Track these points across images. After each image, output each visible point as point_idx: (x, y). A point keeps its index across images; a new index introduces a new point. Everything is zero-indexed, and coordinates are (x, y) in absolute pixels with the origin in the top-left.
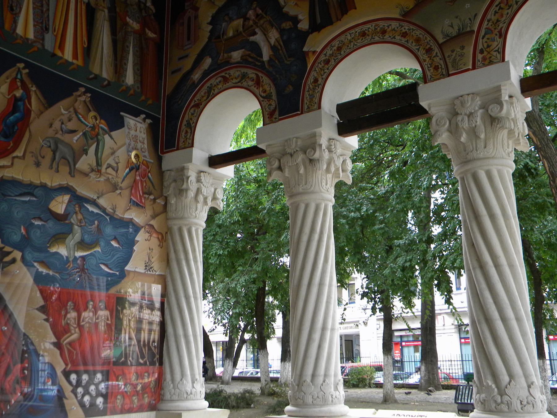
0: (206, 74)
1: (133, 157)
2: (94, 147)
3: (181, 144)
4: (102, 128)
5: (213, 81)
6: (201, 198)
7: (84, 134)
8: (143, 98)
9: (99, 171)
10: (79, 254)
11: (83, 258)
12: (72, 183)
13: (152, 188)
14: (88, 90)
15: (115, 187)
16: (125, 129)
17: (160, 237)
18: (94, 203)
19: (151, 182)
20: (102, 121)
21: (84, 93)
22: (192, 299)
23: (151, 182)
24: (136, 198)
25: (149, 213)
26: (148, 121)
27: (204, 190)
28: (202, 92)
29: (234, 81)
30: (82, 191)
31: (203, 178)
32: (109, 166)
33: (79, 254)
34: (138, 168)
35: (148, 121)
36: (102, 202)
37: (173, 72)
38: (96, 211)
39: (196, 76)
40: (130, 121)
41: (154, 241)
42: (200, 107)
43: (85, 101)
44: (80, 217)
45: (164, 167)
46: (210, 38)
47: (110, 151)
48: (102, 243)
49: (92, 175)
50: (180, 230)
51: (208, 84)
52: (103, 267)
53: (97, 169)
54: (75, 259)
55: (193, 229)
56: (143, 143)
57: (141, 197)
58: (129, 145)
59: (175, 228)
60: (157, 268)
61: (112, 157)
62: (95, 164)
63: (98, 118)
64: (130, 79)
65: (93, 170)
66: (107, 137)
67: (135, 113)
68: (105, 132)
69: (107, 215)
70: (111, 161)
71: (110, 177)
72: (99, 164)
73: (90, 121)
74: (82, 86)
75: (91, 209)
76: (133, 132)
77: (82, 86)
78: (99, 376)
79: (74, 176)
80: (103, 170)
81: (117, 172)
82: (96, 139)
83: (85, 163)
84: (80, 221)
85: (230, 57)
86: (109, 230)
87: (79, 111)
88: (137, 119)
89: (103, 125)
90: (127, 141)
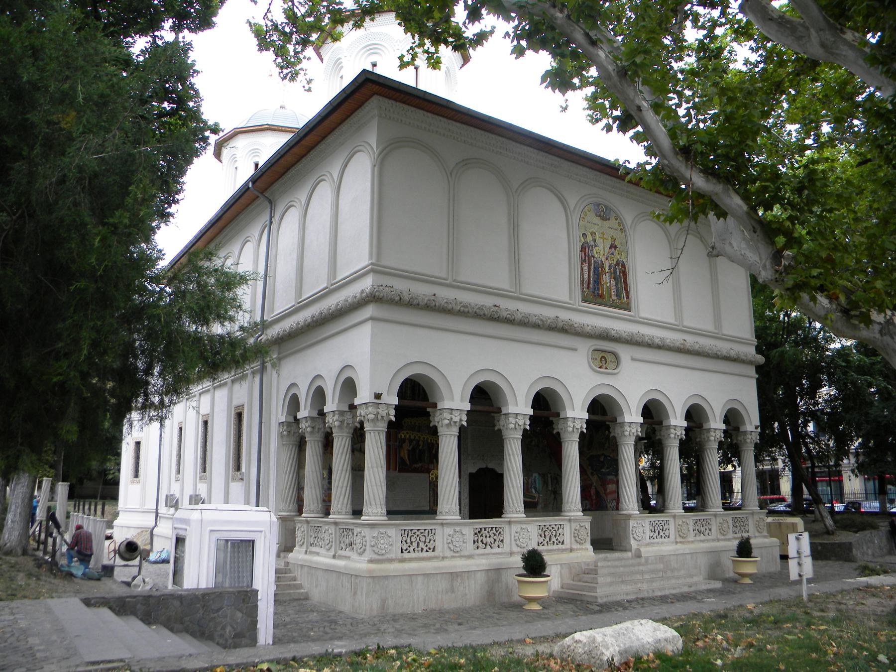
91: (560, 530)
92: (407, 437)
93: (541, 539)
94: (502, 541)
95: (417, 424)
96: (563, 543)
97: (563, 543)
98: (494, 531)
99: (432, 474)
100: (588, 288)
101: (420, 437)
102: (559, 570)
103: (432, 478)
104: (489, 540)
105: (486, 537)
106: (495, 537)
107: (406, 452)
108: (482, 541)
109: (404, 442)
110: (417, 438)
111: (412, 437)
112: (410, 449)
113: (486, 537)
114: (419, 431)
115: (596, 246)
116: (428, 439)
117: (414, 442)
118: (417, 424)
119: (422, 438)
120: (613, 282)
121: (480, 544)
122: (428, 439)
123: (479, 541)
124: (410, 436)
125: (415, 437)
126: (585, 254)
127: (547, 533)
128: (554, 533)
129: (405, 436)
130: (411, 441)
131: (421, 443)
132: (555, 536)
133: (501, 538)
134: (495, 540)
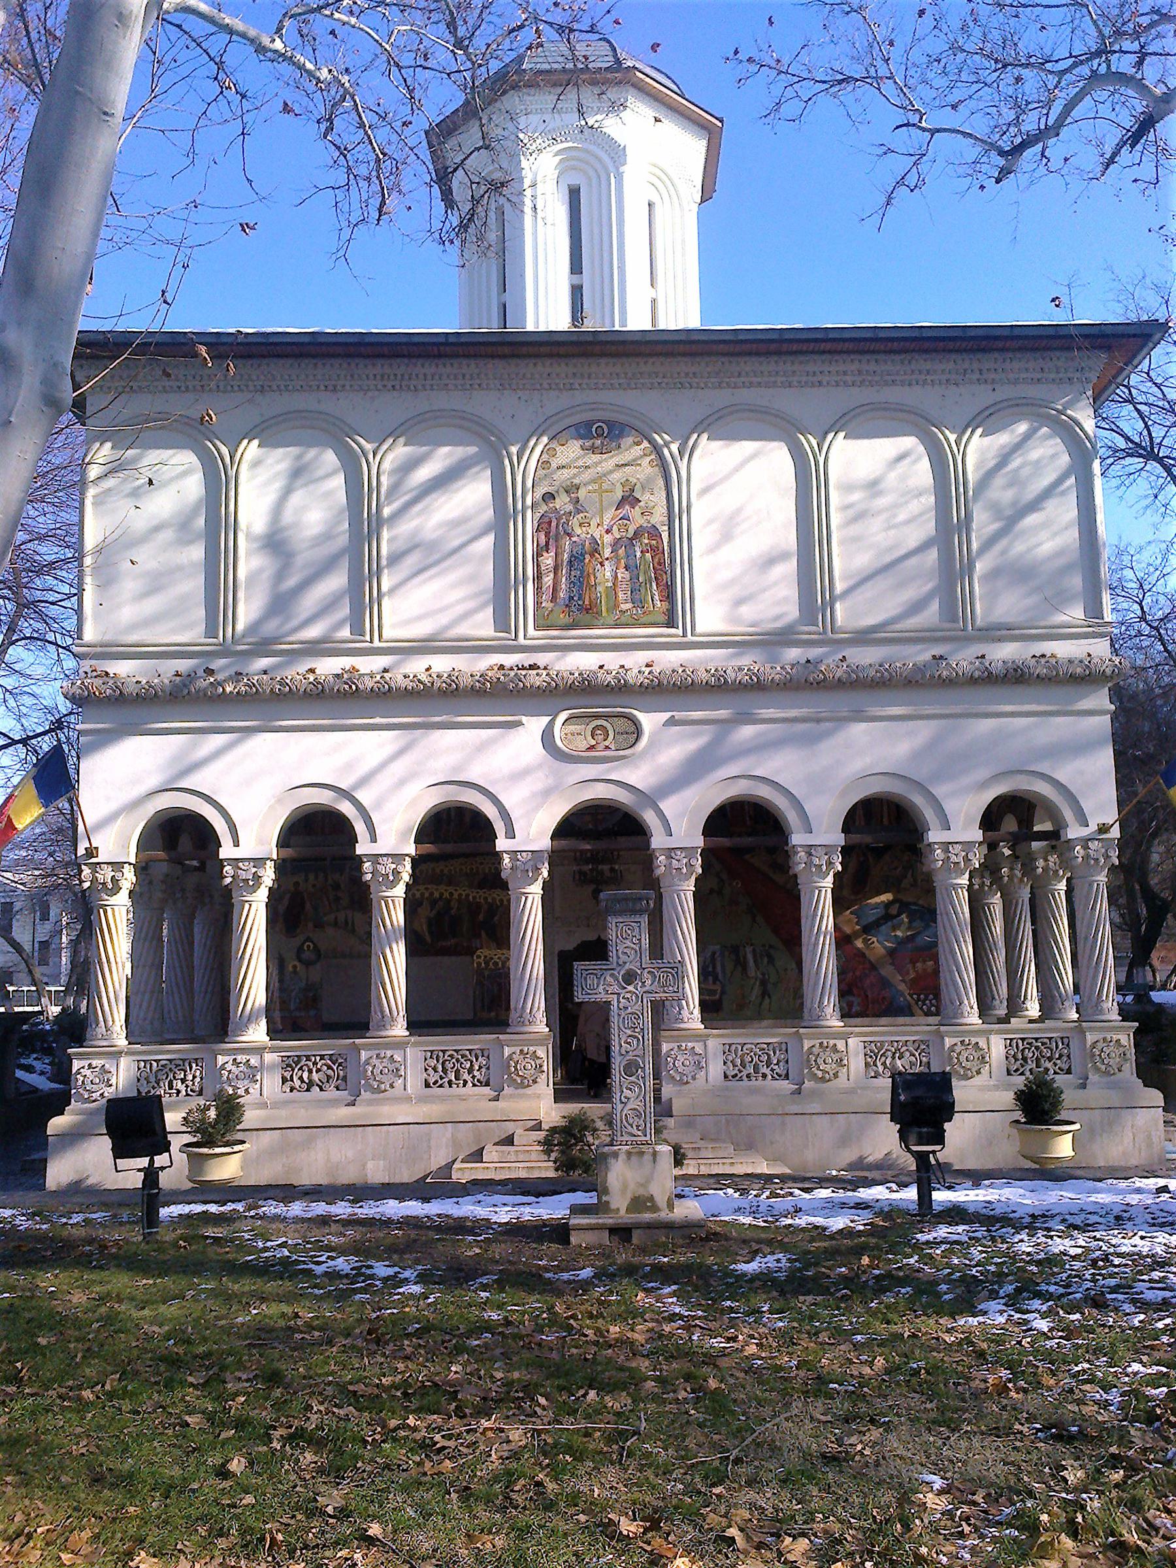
12: (900, 896)
18: (915, 904)
30: (905, 899)
36: (921, 902)
72: (915, 881)
78: (931, 996)
83: (905, 883)
92: (427, 895)
94: (345, 1079)
99: (479, 957)
100: (554, 598)
101: (451, 894)
102: (449, 1135)
103: (479, 964)
106: (330, 1072)
107: (423, 920)
109: (421, 904)
110: (446, 895)
111: (437, 895)
112: (432, 915)
114: (450, 883)
115: (579, 512)
116: (467, 895)
117: (441, 903)
118: (446, 871)
119: (456, 896)
120: (622, 574)
122: (467, 895)
124: (432, 894)
125: (441, 894)
126: (547, 535)
127: (449, 1065)
129: (422, 894)
130: (434, 903)
131: (454, 904)
132: (470, 1071)
134: (329, 1077)
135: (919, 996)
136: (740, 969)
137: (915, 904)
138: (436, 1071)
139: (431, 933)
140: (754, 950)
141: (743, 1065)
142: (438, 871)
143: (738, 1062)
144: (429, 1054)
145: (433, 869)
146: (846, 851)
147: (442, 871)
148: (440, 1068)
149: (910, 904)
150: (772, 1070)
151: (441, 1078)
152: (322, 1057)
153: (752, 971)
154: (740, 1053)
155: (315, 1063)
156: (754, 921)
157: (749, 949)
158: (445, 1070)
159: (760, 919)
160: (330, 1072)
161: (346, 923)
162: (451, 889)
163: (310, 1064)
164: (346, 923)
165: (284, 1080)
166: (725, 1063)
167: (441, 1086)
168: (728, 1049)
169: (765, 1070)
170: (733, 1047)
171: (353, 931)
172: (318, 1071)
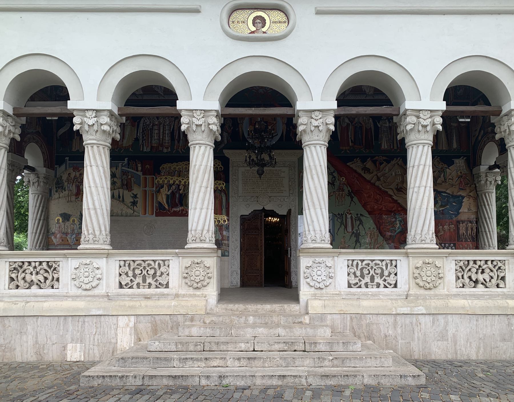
0: (482, 137)
1: (459, 173)
2: (442, 175)
3: (478, 164)
4: (445, 167)
5: (485, 139)
6: (488, 182)
7: (439, 171)
8: (462, 150)
9: (446, 182)
10: (441, 209)
11: (442, 210)
13: (468, 182)
14: (438, 156)
15: (452, 185)
16: (455, 164)
17: (474, 198)
19: (469, 180)
20: (445, 165)
21: (437, 158)
22: (488, 219)
23: (469, 180)
24: (462, 187)
25: (468, 191)
26: (465, 158)
27: (489, 179)
28: (482, 144)
29: (491, 139)
31: (488, 175)
32: (450, 179)
33: (441, 209)
34: (462, 177)
35: (465, 158)
37: (474, 136)
38: (446, 195)
39: (480, 138)
40: (456, 161)
41: (471, 200)
42: (482, 149)
43: (438, 161)
44: (440, 198)
45: (474, 173)
46: (482, 123)
47: (449, 174)
48: (449, 204)
49: (443, 184)
50: (482, 195)
51: (484, 141)
52: (450, 212)
53: (445, 181)
54: (440, 211)
55: (490, 194)
56: (463, 167)
57: (464, 186)
58: (457, 169)
59: (480, 195)
60: (474, 209)
61: (450, 176)
62: (444, 180)
63: (443, 164)
64: (455, 146)
65: (443, 182)
66: (447, 169)
67: (458, 157)
68: (447, 168)
69: (450, 195)
70: (450, 177)
71: (450, 182)
73: (441, 166)
74: (436, 156)
75: (444, 194)
76: (458, 165)
77: (436, 156)
79: (436, 186)
80: (447, 181)
81: (453, 180)
82: (443, 172)
84: (440, 199)
85: (488, 130)
86: (451, 200)
87: (436, 164)
88: (460, 159)
89: (446, 166)
90: (456, 168)
91: (163, 269)
93: (125, 280)
94: (58, 280)
95: (177, 169)
96: (167, 286)
97: (167, 286)
98: (44, 265)
102: (132, 324)
104: (34, 277)
105: (31, 273)
106: (46, 275)
108: (24, 278)
113: (31, 273)
121: (21, 283)
123: (20, 278)
127: (137, 272)
128: (152, 272)
130: (170, 186)
133: (56, 276)
134: (46, 279)
135: (445, 244)
136: (343, 227)
137: (445, 192)
138: (128, 276)
139: (167, 202)
140: (351, 217)
141: (362, 276)
142: (172, 168)
143: (358, 273)
144: (122, 263)
145: (170, 168)
146: (445, 116)
147: (175, 168)
148: (130, 273)
149: (443, 192)
150: (385, 280)
151: (131, 281)
152: (41, 263)
153: (350, 229)
154: (360, 267)
155: (35, 267)
156: (352, 200)
157: (349, 216)
158: (135, 276)
159: (355, 199)
160: (46, 275)
161: (119, 197)
162: (180, 179)
163: (31, 269)
164: (119, 197)
165: (12, 279)
166: (349, 274)
167: (131, 287)
168: (351, 264)
169: (377, 280)
170: (355, 263)
171: (123, 201)
172: (37, 273)
